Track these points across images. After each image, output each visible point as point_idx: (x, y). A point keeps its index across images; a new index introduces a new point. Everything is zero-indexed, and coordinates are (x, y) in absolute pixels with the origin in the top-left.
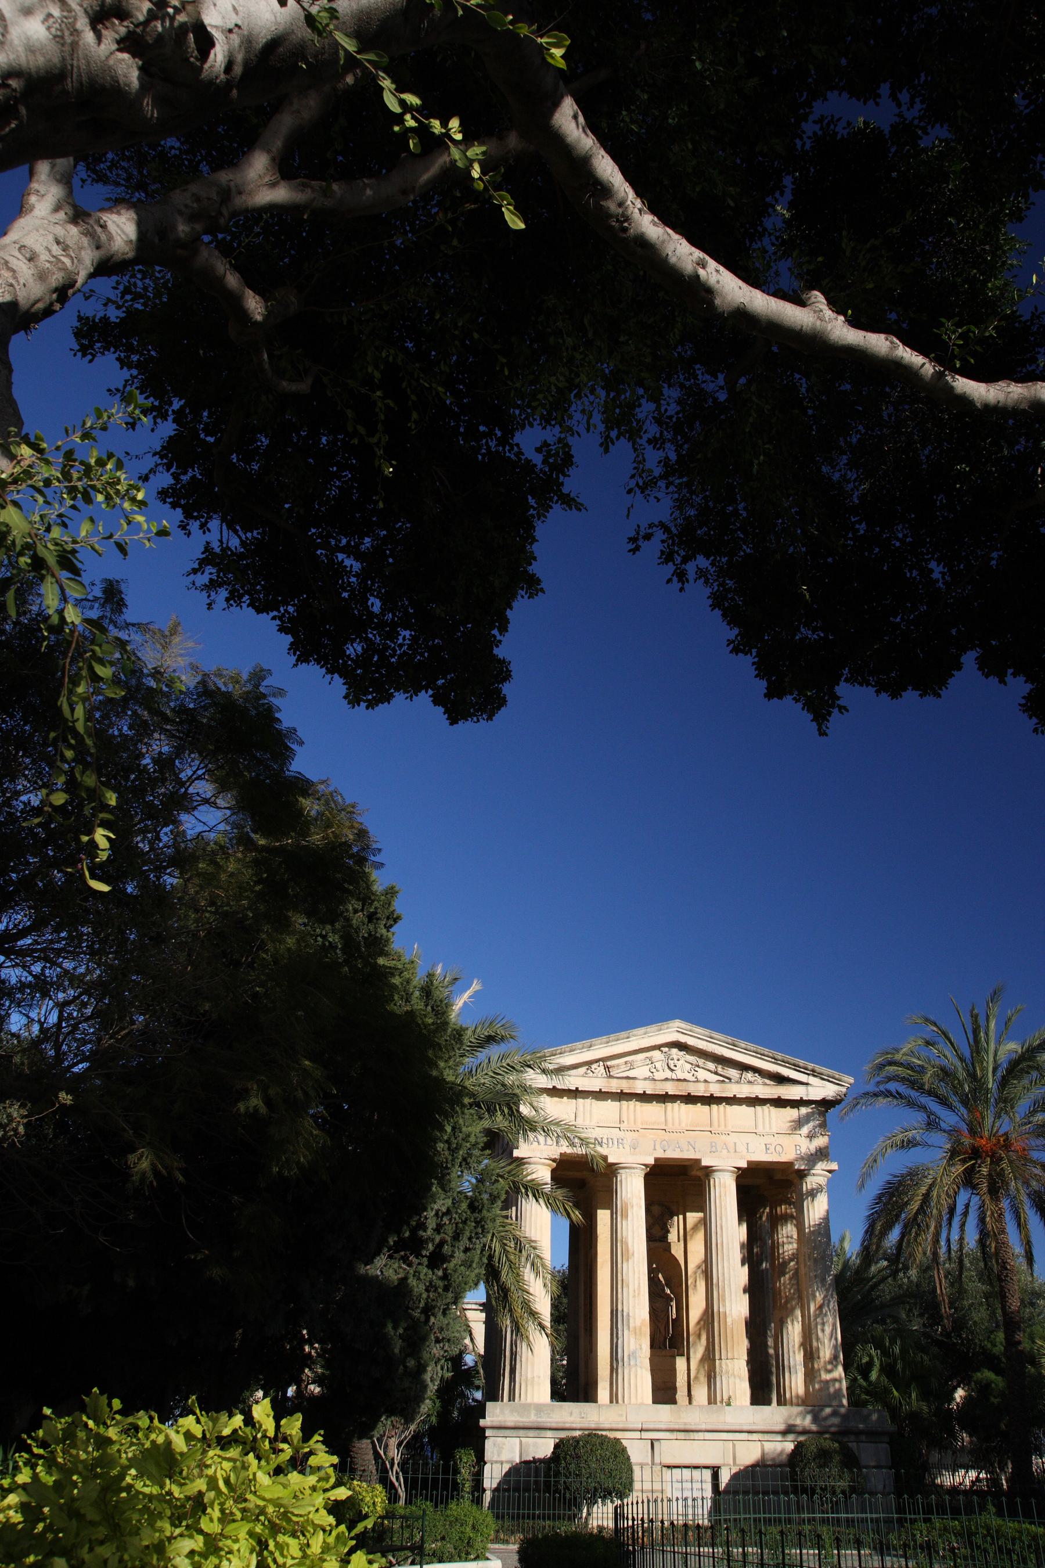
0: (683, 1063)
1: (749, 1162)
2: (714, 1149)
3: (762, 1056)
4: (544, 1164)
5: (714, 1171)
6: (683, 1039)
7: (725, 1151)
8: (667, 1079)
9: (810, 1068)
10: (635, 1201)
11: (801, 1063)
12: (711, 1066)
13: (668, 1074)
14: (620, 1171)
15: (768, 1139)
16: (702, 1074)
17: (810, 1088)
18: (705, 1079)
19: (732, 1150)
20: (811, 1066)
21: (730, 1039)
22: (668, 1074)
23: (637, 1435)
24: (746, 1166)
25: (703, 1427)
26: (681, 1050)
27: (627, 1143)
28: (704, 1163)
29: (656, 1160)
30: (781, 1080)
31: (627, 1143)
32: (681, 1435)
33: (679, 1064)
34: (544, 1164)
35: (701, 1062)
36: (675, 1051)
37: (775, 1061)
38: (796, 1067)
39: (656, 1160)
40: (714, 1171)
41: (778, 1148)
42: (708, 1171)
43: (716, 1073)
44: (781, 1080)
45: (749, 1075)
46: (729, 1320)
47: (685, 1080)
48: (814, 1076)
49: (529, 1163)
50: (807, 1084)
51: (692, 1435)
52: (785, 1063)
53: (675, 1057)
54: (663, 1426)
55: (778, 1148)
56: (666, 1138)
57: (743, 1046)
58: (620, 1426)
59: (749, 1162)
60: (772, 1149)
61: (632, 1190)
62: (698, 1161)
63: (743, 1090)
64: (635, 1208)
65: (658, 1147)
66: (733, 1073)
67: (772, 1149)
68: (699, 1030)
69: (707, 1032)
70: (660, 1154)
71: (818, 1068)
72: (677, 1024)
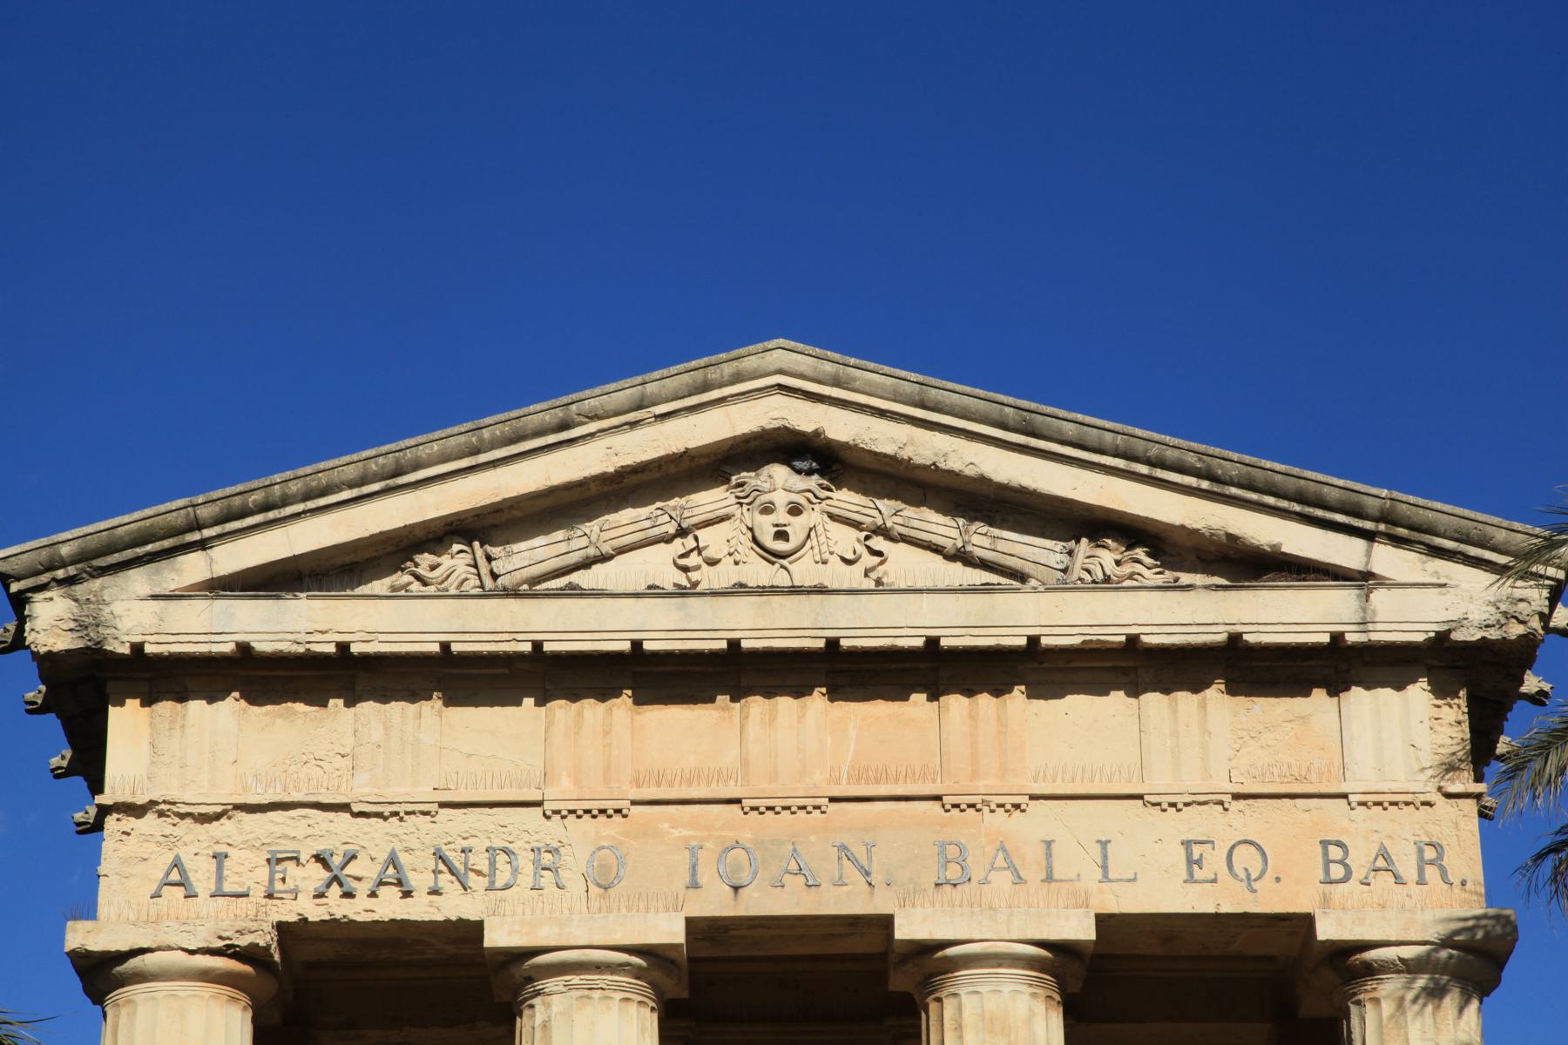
0: (828, 529)
1: (1102, 921)
2: (953, 872)
4: (206, 976)
6: (804, 418)
7: (1002, 880)
8: (740, 589)
9: (1372, 504)
11: (1334, 485)
13: (760, 572)
14: (552, 984)
15: (1198, 822)
16: (904, 563)
17: (1379, 597)
18: (921, 594)
19: (1034, 874)
20: (1376, 495)
21: (1010, 404)
22: (760, 572)
27: (574, 866)
28: (904, 930)
31: (574, 866)
33: (797, 527)
34: (206, 976)
35: (887, 510)
36: (779, 480)
37: (1217, 487)
38: (1310, 508)
39: (690, 923)
41: (1246, 858)
42: (931, 964)
43: (962, 557)
45: (1107, 557)
47: (821, 590)
48: (1398, 541)
49: (141, 977)
50: (1364, 579)
53: (781, 499)
55: (1246, 858)
56: (746, 836)
57: (1070, 429)
59: (1102, 921)
62: (885, 923)
65: (706, 875)
67: (1214, 862)
68: (873, 377)
69: (909, 381)
70: (715, 903)
71: (1411, 503)
72: (782, 356)
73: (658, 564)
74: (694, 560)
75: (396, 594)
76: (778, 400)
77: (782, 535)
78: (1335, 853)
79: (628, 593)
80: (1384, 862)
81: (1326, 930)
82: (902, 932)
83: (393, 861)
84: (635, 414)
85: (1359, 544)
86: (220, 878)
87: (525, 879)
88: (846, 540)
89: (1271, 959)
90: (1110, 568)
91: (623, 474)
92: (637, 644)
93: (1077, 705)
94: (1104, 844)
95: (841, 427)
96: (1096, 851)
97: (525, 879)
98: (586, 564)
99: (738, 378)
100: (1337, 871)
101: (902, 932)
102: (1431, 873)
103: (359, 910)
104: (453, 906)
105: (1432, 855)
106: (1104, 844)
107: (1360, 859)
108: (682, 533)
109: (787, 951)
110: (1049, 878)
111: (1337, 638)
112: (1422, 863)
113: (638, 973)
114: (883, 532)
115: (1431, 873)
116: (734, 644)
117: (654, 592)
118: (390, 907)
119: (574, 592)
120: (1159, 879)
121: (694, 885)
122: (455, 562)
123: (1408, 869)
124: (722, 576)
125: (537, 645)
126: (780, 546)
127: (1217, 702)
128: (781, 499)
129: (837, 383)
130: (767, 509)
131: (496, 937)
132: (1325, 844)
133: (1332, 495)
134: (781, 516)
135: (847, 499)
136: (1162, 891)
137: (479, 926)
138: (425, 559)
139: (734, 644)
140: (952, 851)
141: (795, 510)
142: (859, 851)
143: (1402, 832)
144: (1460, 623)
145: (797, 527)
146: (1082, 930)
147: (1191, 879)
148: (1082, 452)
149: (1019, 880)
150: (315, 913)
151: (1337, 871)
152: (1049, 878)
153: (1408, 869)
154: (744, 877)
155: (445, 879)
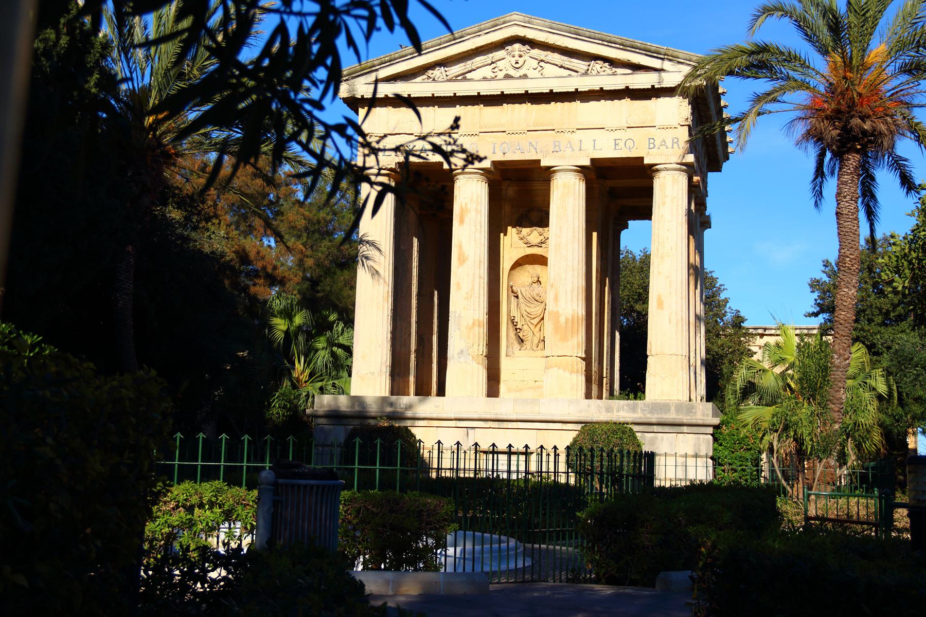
1: (592, 160)
2: (557, 149)
3: (610, 43)
5: (555, 172)
6: (521, 32)
7: (569, 150)
9: (663, 51)
12: (557, 58)
15: (618, 135)
16: (549, 70)
17: (663, 74)
18: (552, 75)
23: (453, 423)
25: (514, 417)
26: (524, 45)
30: (637, 68)
32: (496, 424)
33: (521, 61)
36: (517, 46)
37: (625, 47)
38: (649, 52)
40: (555, 172)
41: (629, 143)
43: (561, 67)
44: (637, 68)
45: (597, 66)
46: (562, 320)
48: (670, 60)
51: (506, 425)
52: (633, 48)
54: (475, 417)
56: (507, 141)
57: (587, 34)
58: (434, 416)
59: (592, 160)
60: (621, 144)
61: (470, 198)
63: (585, 84)
66: (580, 65)
67: (621, 144)
70: (499, 157)
71: (672, 50)
72: (516, 17)
73: (487, 72)
74: (496, 70)
75: (423, 82)
76: (516, 28)
77: (517, 63)
78: (652, 141)
79: (482, 78)
81: (646, 162)
82: (542, 164)
84: (477, 34)
85: (660, 61)
88: (534, 63)
90: (599, 70)
91: (477, 49)
93: (593, 104)
95: (531, 34)
98: (470, 72)
99: (504, 23)
101: (542, 164)
102: (675, 145)
105: (675, 141)
107: (657, 143)
108: (493, 63)
111: (653, 86)
112: (673, 143)
113: (481, 174)
114: (542, 61)
115: (675, 145)
116: (502, 92)
117: (485, 79)
119: (465, 79)
120: (608, 148)
122: (437, 72)
124: (501, 75)
126: (517, 66)
127: (626, 102)
128: (517, 53)
129: (529, 23)
130: (514, 56)
133: (653, 49)
134: (517, 58)
135: (536, 52)
136: (608, 150)
138: (430, 72)
139: (502, 92)
140: (557, 143)
141: (520, 56)
142: (534, 144)
143: (669, 135)
145: (521, 61)
146: (587, 163)
147: (615, 149)
148: (591, 38)
151: (652, 146)
153: (669, 144)
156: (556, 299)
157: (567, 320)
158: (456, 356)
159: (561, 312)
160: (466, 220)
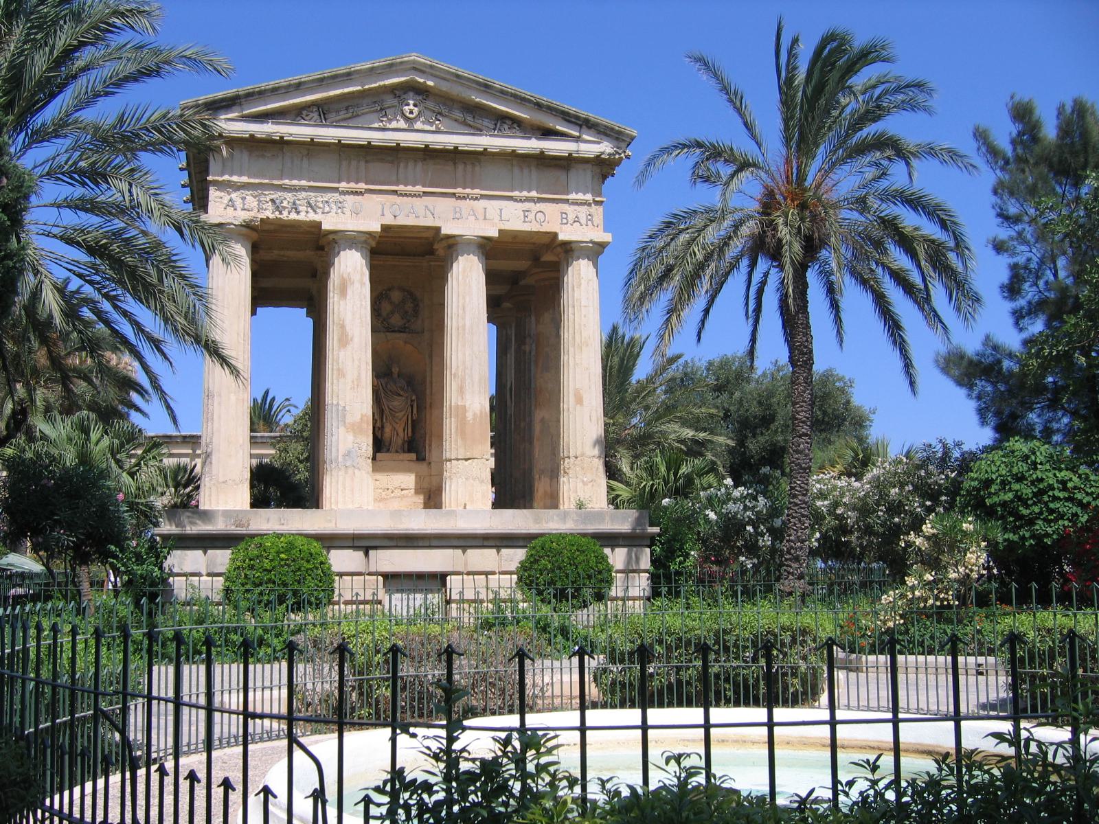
1: (500, 231)
2: (458, 215)
10: (356, 277)
19: (481, 217)
24: (496, 234)
28: (444, 231)
29: (385, 228)
38: (567, 117)
39: (382, 225)
44: (547, 133)
46: (469, 415)
59: (500, 231)
62: (438, 229)
64: (357, 285)
67: (531, 216)
70: (389, 220)
78: (564, 216)
80: (577, 220)
81: (562, 237)
83: (294, 203)
86: (244, 204)
87: (334, 211)
89: (534, 244)
92: (369, 143)
94: (501, 210)
96: (499, 212)
97: (334, 211)
100: (565, 221)
103: (285, 216)
104: (312, 217)
105: (590, 217)
106: (501, 210)
107: (571, 217)
108: (381, 110)
109: (407, 235)
110: (485, 219)
118: (293, 216)
121: (383, 215)
123: (583, 221)
125: (340, 141)
126: (411, 116)
131: (325, 227)
132: (562, 213)
134: (411, 107)
135: (429, 104)
137: (321, 223)
144: (602, 153)
146: (494, 233)
149: (477, 219)
150: (271, 216)
152: (485, 219)
153: (583, 221)
154: (397, 213)
155: (309, 209)
156: (461, 390)
157: (475, 415)
158: (340, 459)
159: (467, 406)
160: (349, 292)
